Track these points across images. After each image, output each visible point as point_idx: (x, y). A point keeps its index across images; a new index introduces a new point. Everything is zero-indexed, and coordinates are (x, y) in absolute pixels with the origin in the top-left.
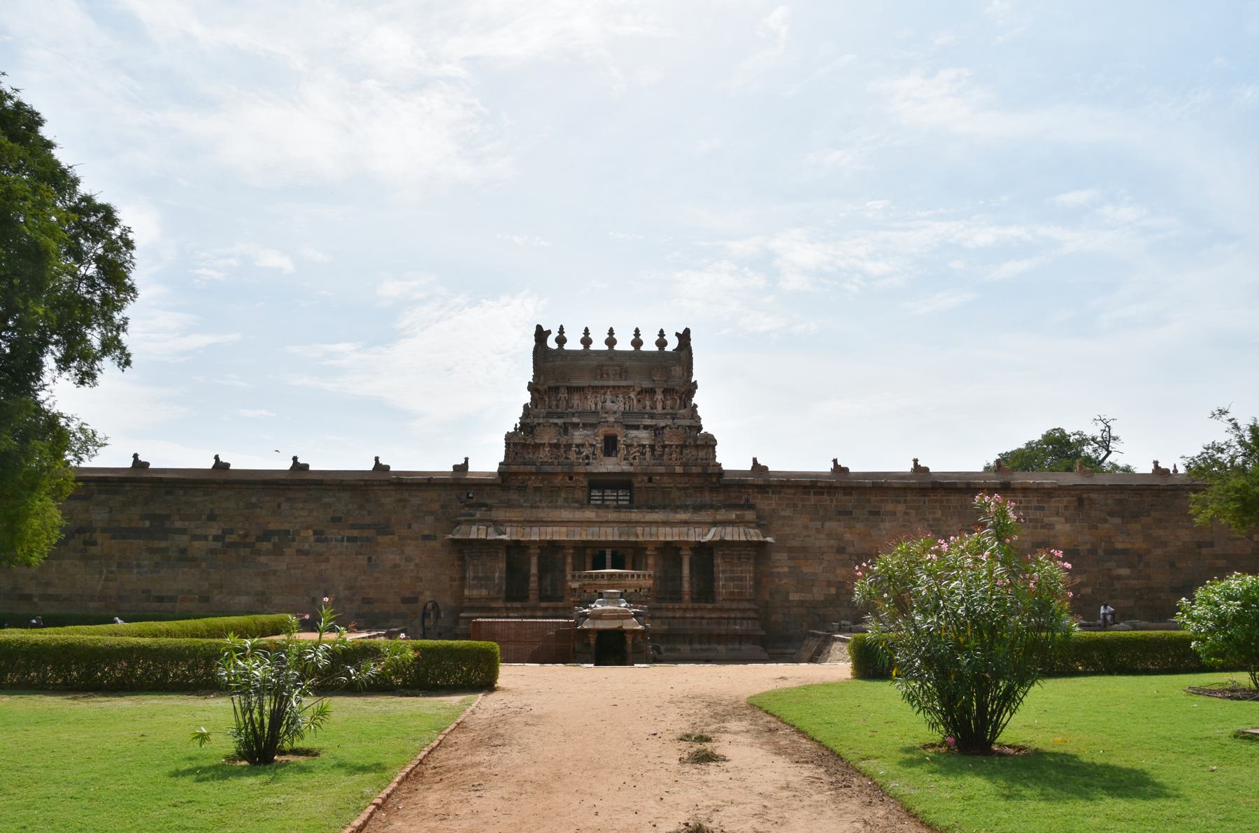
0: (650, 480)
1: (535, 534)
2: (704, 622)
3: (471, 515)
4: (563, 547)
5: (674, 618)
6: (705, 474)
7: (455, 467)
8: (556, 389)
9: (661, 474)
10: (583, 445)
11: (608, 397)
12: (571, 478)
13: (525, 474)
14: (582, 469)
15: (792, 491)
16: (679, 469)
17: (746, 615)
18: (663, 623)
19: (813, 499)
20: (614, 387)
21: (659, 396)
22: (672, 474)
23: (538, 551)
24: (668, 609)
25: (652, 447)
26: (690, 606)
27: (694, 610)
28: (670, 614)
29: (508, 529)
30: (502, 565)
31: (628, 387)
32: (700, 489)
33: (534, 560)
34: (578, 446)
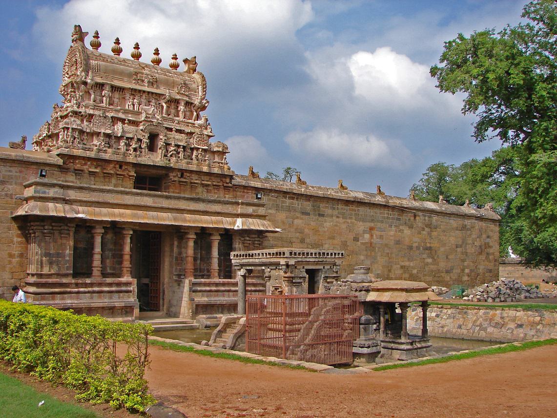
0: (182, 176)
1: (106, 215)
2: (231, 294)
3: (45, 193)
4: (124, 228)
5: (210, 291)
6: (222, 176)
7: (14, 146)
8: (100, 86)
9: (191, 172)
10: (132, 139)
11: (143, 100)
12: (121, 167)
13: (84, 158)
14: (131, 159)
15: (276, 195)
16: (205, 169)
17: (258, 288)
18: (203, 296)
19: (288, 201)
20: (149, 92)
21: (181, 108)
22: (199, 173)
23: (103, 231)
24: (205, 284)
25: (184, 147)
26: (221, 280)
27: (224, 284)
28: (208, 288)
29: (80, 208)
30: (72, 243)
31: (160, 95)
32: (217, 187)
33: (98, 240)
34: (128, 138)
